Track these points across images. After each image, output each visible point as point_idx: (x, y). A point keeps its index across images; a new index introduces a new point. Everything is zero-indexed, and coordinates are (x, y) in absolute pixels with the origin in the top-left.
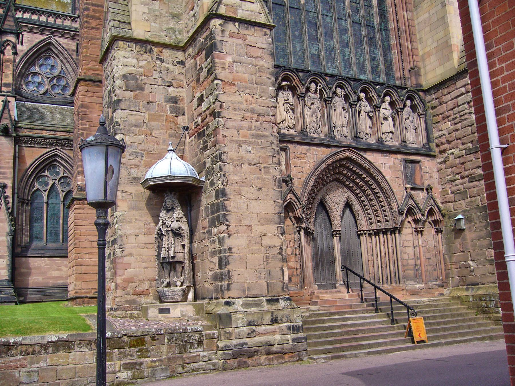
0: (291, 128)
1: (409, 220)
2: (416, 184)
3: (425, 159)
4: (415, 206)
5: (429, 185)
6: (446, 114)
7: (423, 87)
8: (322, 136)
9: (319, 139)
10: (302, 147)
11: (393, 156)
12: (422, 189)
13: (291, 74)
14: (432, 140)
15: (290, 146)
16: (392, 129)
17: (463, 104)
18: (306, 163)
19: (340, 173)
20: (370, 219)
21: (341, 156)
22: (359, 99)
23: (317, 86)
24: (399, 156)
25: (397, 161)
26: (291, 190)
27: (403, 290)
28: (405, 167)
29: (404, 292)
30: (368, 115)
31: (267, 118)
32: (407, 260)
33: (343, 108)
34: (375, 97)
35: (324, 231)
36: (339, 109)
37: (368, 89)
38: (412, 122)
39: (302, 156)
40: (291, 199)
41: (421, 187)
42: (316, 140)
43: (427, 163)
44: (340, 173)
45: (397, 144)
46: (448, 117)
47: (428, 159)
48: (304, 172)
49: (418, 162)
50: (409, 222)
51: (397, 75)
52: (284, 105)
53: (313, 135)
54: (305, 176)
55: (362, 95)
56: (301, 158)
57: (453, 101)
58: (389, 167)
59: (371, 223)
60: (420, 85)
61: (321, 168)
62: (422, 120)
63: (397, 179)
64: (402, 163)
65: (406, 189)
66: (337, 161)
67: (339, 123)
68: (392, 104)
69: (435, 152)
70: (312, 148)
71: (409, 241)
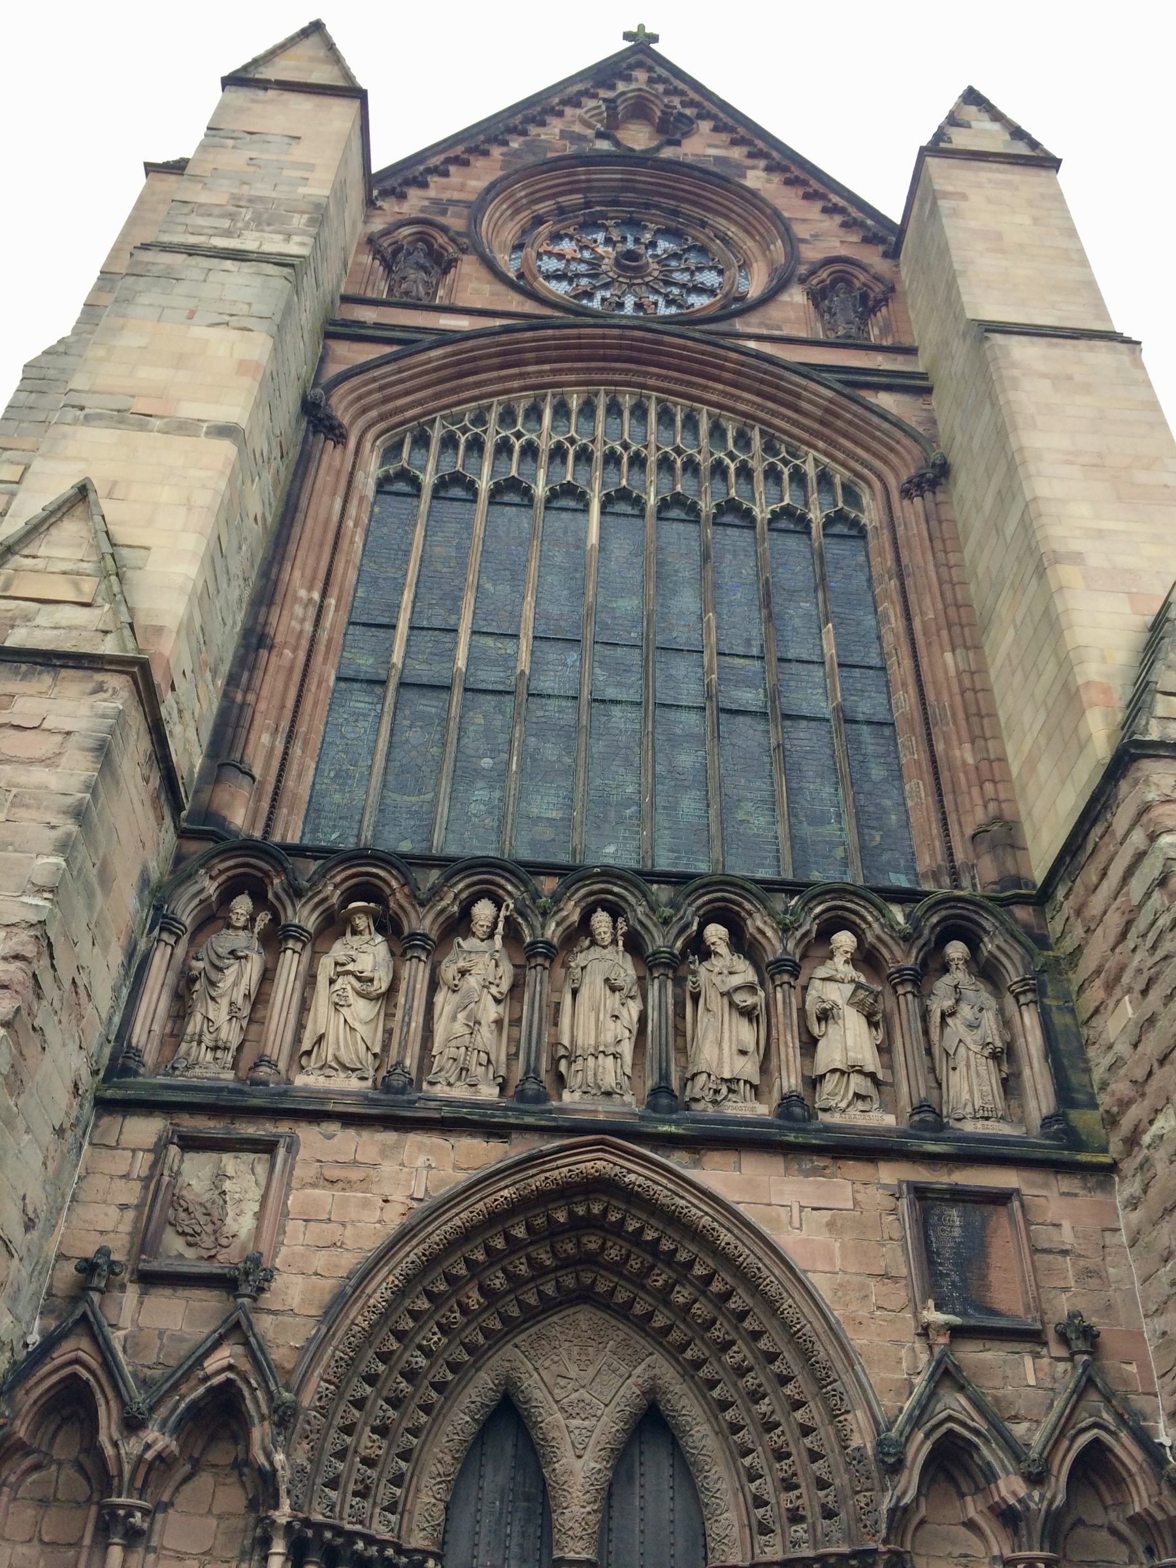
0: (345, 1068)
1: (972, 1513)
2: (992, 1312)
3: (1046, 1186)
4: (981, 1425)
5: (1072, 1316)
6: (1111, 965)
7: (1034, 886)
8: (489, 1093)
9: (475, 1105)
10: (366, 1135)
11: (857, 1170)
12: (1031, 1337)
13: (374, 870)
14: (1080, 1097)
15: (309, 1136)
16: (870, 1061)
17: (1148, 895)
18: (365, 1204)
19: (590, 1260)
20: (760, 1502)
21: (560, 1172)
23: (499, 910)
24: (890, 1174)
25: (876, 1198)
26: (238, 1325)
28: (925, 1226)
30: (732, 1004)
33: (607, 980)
34: (770, 933)
36: (593, 988)
37: (740, 905)
38: (972, 1026)
39: (355, 1175)
40: (230, 1368)
41: (1030, 1322)
42: (432, 1104)
44: (590, 1260)
45: (890, 1120)
46: (1118, 978)
47: (1066, 1184)
48: (349, 1244)
49: (1001, 1198)
50: (971, 1525)
51: (925, 862)
52: (332, 982)
53: (440, 1091)
54: (348, 1261)
55: (716, 933)
56: (349, 1184)
57: (1120, 899)
58: (831, 1225)
59: (765, 1530)
60: (1017, 881)
61: (438, 1233)
62: (1030, 1019)
63: (872, 1283)
64: (904, 1203)
65: (925, 1331)
66: (543, 1198)
67: (586, 1038)
68: (866, 958)
69: (1104, 1150)
70: (414, 1139)
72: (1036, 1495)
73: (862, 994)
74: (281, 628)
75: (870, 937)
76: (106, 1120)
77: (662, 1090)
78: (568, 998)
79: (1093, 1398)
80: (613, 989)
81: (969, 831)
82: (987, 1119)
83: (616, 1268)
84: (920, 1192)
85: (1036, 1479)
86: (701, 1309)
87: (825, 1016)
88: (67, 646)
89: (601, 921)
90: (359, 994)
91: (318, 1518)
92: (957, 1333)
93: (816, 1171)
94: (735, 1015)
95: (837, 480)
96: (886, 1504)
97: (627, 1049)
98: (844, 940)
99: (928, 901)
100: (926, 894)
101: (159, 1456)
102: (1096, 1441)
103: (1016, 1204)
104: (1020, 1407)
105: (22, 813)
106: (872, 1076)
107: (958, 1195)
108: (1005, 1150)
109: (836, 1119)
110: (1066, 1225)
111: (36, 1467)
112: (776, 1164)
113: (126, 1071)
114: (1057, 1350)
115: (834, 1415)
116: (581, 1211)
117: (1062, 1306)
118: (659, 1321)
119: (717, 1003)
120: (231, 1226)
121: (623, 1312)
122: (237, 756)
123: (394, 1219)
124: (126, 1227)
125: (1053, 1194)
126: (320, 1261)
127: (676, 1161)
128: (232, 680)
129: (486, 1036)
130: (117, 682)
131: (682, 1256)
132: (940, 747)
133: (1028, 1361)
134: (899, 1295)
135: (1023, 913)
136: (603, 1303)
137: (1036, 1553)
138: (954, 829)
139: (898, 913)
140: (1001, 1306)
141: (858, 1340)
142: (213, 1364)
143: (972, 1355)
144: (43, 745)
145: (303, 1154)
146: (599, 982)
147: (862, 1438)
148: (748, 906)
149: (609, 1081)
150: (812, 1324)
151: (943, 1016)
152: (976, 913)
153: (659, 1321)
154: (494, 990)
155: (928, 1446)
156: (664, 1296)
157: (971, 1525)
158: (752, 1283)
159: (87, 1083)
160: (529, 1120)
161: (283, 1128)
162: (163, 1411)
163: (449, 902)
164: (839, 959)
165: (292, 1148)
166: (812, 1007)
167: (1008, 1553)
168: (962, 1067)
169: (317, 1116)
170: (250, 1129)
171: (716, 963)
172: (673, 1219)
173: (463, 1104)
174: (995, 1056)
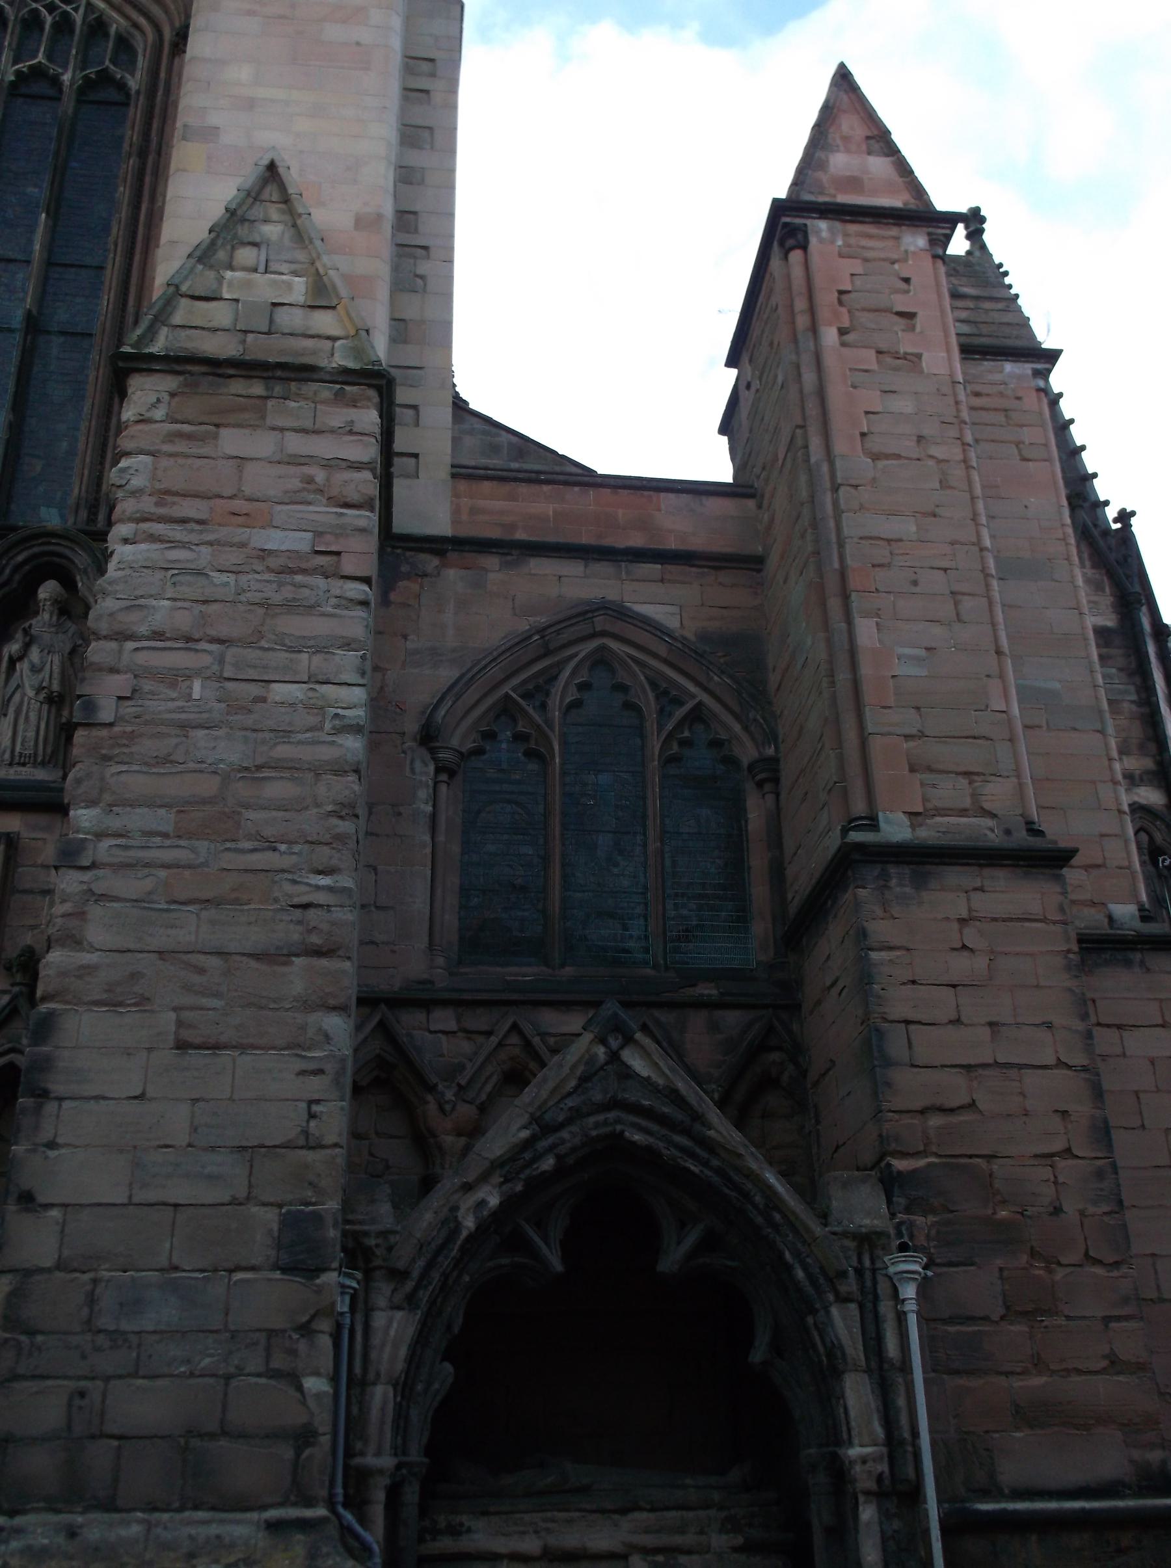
38: (35, 670)
82: (24, 765)
95: (113, 30)
99: (13, 537)
151: (11, 658)
152: (73, 549)
174: (50, 700)
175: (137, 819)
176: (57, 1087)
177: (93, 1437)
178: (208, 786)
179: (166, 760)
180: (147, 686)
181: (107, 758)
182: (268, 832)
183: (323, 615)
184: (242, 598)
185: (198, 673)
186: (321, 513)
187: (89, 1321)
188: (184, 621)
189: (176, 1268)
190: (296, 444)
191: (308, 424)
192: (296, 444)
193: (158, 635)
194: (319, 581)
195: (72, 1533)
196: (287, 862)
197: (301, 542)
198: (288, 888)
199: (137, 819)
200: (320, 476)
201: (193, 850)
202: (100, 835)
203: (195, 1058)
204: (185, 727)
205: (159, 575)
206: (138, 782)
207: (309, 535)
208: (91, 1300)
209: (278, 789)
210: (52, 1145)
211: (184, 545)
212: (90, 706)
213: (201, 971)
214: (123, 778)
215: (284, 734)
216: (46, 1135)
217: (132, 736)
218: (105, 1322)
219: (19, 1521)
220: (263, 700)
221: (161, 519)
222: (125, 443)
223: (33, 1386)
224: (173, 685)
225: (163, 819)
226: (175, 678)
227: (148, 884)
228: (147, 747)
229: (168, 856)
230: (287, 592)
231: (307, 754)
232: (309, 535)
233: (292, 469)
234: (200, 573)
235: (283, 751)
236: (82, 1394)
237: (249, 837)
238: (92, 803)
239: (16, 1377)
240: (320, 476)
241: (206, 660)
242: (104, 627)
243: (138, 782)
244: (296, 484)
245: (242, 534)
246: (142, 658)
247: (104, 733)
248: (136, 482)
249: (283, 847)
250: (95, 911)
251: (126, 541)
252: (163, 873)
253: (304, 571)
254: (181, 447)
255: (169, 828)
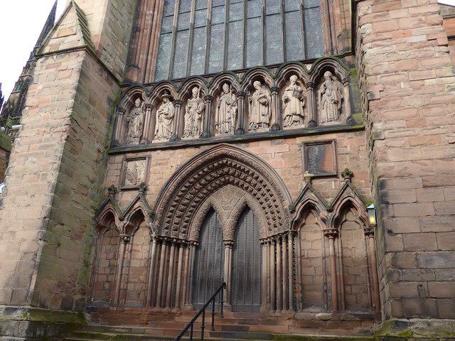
4: (317, 200)
5: (347, 170)
8: (197, 137)
10: (166, 152)
12: (336, 176)
15: (153, 154)
21: (213, 154)
22: (252, 89)
24: (299, 140)
25: (297, 147)
27: (289, 319)
29: (290, 322)
31: (59, 129)
32: (313, 277)
34: (270, 80)
35: (216, 242)
36: (223, 105)
43: (347, 142)
45: (303, 126)
47: (350, 135)
49: (329, 142)
50: (317, 223)
53: (185, 139)
54: (164, 181)
55: (257, 83)
58: (282, 157)
62: (346, 90)
71: (317, 250)
72: (330, 215)
73: (296, 93)
74: (142, 24)
75: (300, 76)
76: (111, 158)
77: (241, 129)
78: (217, 109)
79: (349, 189)
80: (228, 105)
81: (337, 35)
83: (233, 175)
84: (307, 144)
85: (330, 211)
86: (254, 181)
87: (287, 101)
88: (71, 47)
89: (225, 86)
90: (167, 118)
91: (163, 235)
92: (313, 178)
93: (279, 143)
94: (261, 105)
96: (290, 221)
97: (233, 120)
98: (293, 78)
100: (315, 59)
101: (128, 225)
102: (349, 200)
103: (333, 143)
104: (330, 194)
105: (64, 91)
106: (299, 115)
107: (317, 143)
108: (332, 129)
109: (288, 128)
110: (349, 146)
111: (108, 230)
112: (268, 142)
113: (114, 146)
114: (341, 179)
115: (282, 201)
116: (220, 162)
117: (342, 169)
118: (245, 186)
119: (257, 103)
120: (139, 177)
121: (237, 184)
122: (133, 63)
123: (174, 171)
124: (118, 180)
125: (346, 139)
126: (158, 182)
127: (242, 146)
128: (131, 42)
129: (196, 123)
130: (82, 53)
131: (246, 170)
132: (331, 10)
133: (333, 183)
134: (300, 171)
135: (348, 58)
136: (232, 183)
137: (330, 228)
138: (333, 36)
139: (309, 67)
140: (326, 170)
141: (287, 184)
142: (136, 206)
143: (316, 182)
144: (67, 73)
145: (153, 159)
146: (224, 104)
147: (287, 203)
148: (264, 74)
149: (227, 129)
150: (277, 181)
151: (322, 95)
153: (245, 186)
154: (197, 111)
155: (302, 207)
156: (244, 179)
157: (317, 223)
158: (262, 174)
159: (102, 149)
160: (204, 142)
161: (148, 153)
162: (127, 216)
163: (185, 90)
164: (292, 83)
165: (150, 158)
166: (283, 99)
167: (325, 228)
168: (325, 108)
169: (155, 150)
170: (140, 155)
171: (257, 92)
172: (242, 161)
173: (191, 141)
174: (336, 103)
175: (394, 124)
176: (391, 201)
177: (427, 298)
178: (414, 112)
179: (398, 107)
180: (387, 87)
181: (380, 108)
182: (436, 123)
183: (436, 57)
184: (409, 57)
185: (402, 80)
186: (428, 29)
187: (417, 265)
188: (393, 67)
189: (440, 250)
190: (413, 11)
191: (415, 4)
192: (413, 11)
193: (386, 72)
194: (431, 48)
195: (429, 324)
196: (445, 131)
197: (424, 38)
198: (447, 138)
199: (394, 124)
200: (423, 18)
201: (415, 131)
202: (384, 130)
203: (430, 190)
204: (401, 97)
205: (382, 55)
206: (391, 114)
207: (425, 36)
208: (417, 260)
209: (435, 110)
210: (393, 217)
211: (388, 46)
212: (372, 95)
213: (426, 165)
214: (388, 113)
215: (433, 94)
216: (392, 214)
217: (387, 101)
218: (421, 266)
219: (411, 320)
220: (423, 85)
221: (379, 40)
222: (362, 21)
223: (406, 283)
224: (395, 85)
225: (403, 123)
226: (394, 83)
227: (403, 142)
228: (392, 104)
229: (407, 133)
230: (423, 53)
231: (442, 99)
232: (425, 36)
233: (414, 18)
234: (394, 53)
235: (433, 99)
236: (421, 286)
237: (430, 125)
238: (380, 121)
239: (400, 281)
240: (423, 18)
241: (403, 77)
242: (371, 73)
243: (391, 114)
244: (417, 22)
245: (405, 39)
246: (384, 79)
247: (378, 101)
248: (368, 32)
249: (442, 127)
250: (389, 151)
251: (370, 48)
252: (406, 138)
253: (426, 46)
254: (379, 19)
255: (405, 126)
